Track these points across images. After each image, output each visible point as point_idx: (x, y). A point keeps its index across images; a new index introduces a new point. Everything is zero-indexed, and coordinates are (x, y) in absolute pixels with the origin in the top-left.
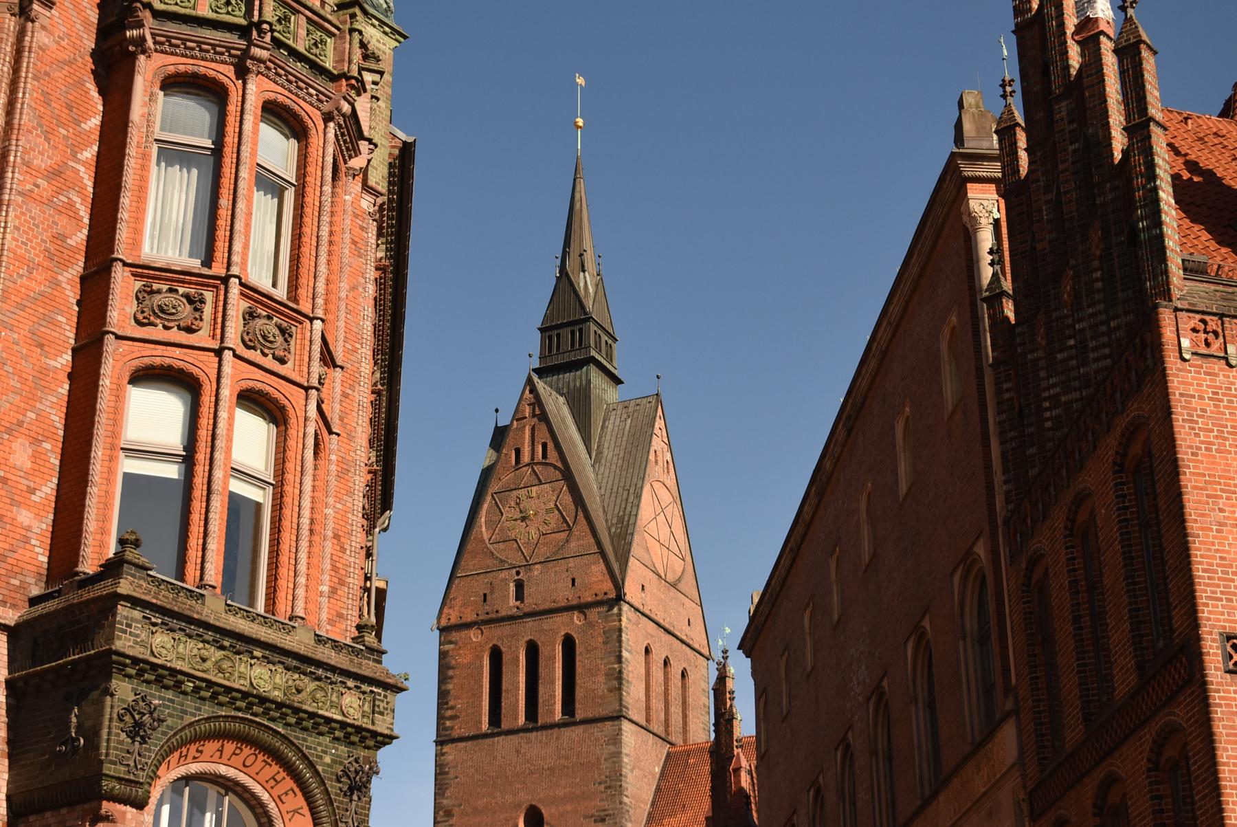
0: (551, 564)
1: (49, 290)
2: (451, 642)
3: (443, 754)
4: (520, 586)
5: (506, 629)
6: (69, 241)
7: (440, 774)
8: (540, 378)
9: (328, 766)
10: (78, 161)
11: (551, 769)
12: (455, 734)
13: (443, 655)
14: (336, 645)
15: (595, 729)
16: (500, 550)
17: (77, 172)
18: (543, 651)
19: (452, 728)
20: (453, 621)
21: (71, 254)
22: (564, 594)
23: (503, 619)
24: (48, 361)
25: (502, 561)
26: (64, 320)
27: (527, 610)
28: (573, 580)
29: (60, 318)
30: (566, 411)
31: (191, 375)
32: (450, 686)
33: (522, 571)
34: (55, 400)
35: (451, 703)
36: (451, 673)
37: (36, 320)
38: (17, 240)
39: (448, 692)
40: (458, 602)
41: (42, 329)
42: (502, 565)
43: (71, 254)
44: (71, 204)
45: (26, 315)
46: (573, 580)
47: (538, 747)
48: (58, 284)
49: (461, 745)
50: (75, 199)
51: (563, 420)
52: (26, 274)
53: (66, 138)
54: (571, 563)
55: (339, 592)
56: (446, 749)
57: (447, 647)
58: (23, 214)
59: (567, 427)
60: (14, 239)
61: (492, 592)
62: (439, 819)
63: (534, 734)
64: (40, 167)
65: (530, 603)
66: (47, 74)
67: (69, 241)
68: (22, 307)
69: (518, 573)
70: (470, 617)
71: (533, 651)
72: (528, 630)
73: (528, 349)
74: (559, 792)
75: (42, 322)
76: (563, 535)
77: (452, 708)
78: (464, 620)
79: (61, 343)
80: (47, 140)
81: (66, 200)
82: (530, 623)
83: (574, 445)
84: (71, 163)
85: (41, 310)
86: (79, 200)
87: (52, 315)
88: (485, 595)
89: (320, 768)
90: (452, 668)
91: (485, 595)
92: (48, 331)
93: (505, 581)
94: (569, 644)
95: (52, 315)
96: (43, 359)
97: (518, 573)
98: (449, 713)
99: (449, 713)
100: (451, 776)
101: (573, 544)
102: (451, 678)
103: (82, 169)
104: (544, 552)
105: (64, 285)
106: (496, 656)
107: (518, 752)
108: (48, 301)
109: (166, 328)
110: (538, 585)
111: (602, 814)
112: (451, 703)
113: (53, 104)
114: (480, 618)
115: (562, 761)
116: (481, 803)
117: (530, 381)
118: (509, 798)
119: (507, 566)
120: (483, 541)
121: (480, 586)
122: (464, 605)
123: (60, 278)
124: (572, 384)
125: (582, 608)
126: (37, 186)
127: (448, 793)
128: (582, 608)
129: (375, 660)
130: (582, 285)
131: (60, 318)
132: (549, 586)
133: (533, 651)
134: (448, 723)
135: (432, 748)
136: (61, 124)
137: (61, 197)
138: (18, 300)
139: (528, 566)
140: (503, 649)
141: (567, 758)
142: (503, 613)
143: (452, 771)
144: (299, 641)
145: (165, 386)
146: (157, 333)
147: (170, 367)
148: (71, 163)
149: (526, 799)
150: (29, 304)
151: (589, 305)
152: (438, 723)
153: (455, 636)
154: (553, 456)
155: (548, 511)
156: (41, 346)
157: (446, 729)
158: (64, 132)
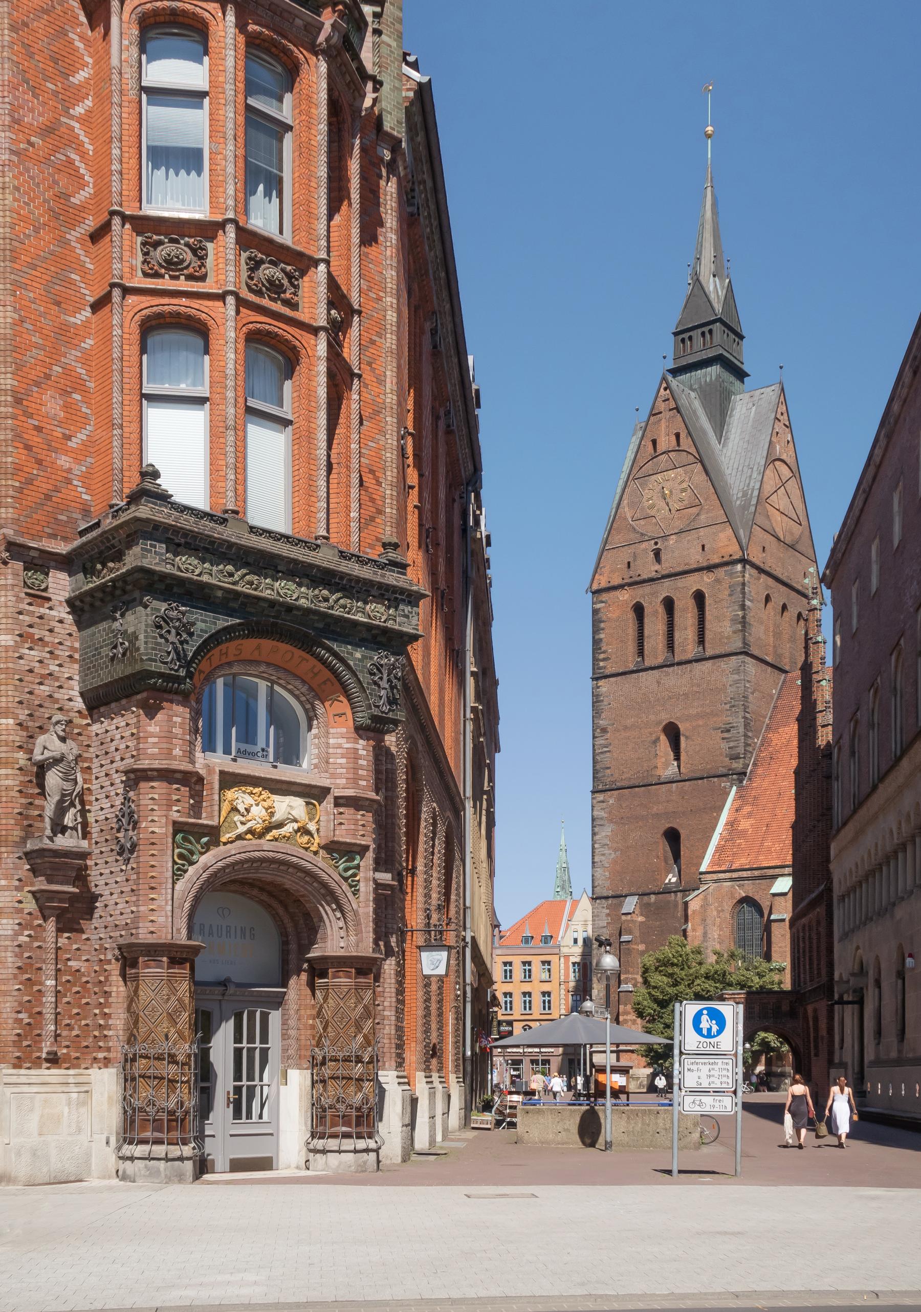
0: (683, 535)
1: (59, 249)
2: (602, 602)
3: (598, 687)
4: (657, 554)
5: (647, 589)
6: (72, 200)
7: (597, 702)
8: (674, 377)
9: (359, 660)
10: (72, 117)
11: (686, 695)
12: (608, 671)
13: (595, 612)
14: (360, 560)
15: (723, 664)
16: (640, 525)
17: (72, 129)
18: (678, 605)
19: (605, 667)
20: (604, 584)
21: (77, 213)
22: (695, 558)
23: (644, 581)
24: (68, 318)
25: (642, 534)
26: (78, 278)
27: (664, 573)
28: (703, 546)
29: (73, 276)
30: (697, 404)
31: (199, 321)
32: (602, 636)
33: (659, 541)
34: (79, 354)
35: (603, 649)
36: (602, 625)
37: (49, 279)
38: (19, 201)
39: (601, 640)
40: (606, 570)
41: (57, 287)
42: (643, 538)
43: (77, 213)
44: (71, 162)
45: (39, 274)
46: (703, 546)
47: (675, 679)
48: (67, 243)
49: (612, 679)
50: (73, 156)
51: (695, 412)
52: (33, 233)
53: (56, 93)
54: (702, 532)
55: (377, 520)
56: (601, 683)
57: (598, 606)
58: (21, 174)
59: (697, 418)
60: (15, 200)
61: (635, 560)
62: (597, 735)
63: (672, 668)
64: (32, 125)
65: (667, 566)
66: (26, 25)
67: (72, 200)
68: (34, 267)
69: (656, 543)
70: (617, 581)
71: (669, 604)
72: (665, 589)
73: (664, 351)
74: (693, 711)
75: (54, 280)
76: (694, 510)
77: (604, 652)
78: (611, 584)
79: (78, 300)
80: (35, 96)
81: (64, 158)
82: (667, 583)
83: (704, 433)
84: (63, 119)
85: (53, 268)
86: (77, 158)
87: (66, 274)
88: (629, 563)
89: (351, 663)
90: (603, 622)
91: (629, 563)
92: (64, 289)
93: (645, 550)
94: (699, 598)
95: (66, 274)
96: (63, 316)
97: (656, 543)
98: (602, 656)
99: (602, 656)
100: (605, 703)
101: (702, 517)
102: (603, 629)
103: (77, 125)
104: (679, 525)
105: (73, 244)
106: (639, 610)
107: (658, 683)
108: (59, 260)
109: (173, 278)
110: (673, 552)
111: (728, 726)
112: (603, 649)
113: (37, 57)
114: (626, 581)
115: (695, 689)
116: (629, 722)
117: (664, 379)
118: (652, 717)
119: (646, 538)
120: (625, 519)
121: (625, 555)
122: (612, 571)
123: (68, 236)
124: (703, 380)
125: (710, 568)
126: (32, 144)
127: (603, 716)
128: (710, 568)
129: (398, 573)
130: (711, 288)
131: (73, 276)
132: (683, 552)
133: (669, 604)
134: (601, 664)
135: (589, 684)
136: (47, 78)
137: (58, 155)
138: (29, 260)
139: (665, 537)
140: (645, 605)
141: (699, 686)
142: (645, 576)
143: (606, 699)
144: (324, 558)
145: (173, 331)
146: (166, 283)
147: (178, 314)
148: (63, 119)
149: (665, 718)
150: (39, 264)
151: (718, 307)
152: (593, 664)
153: (604, 596)
154: (686, 443)
155: (683, 490)
156: (58, 304)
157: (600, 668)
158: (53, 87)
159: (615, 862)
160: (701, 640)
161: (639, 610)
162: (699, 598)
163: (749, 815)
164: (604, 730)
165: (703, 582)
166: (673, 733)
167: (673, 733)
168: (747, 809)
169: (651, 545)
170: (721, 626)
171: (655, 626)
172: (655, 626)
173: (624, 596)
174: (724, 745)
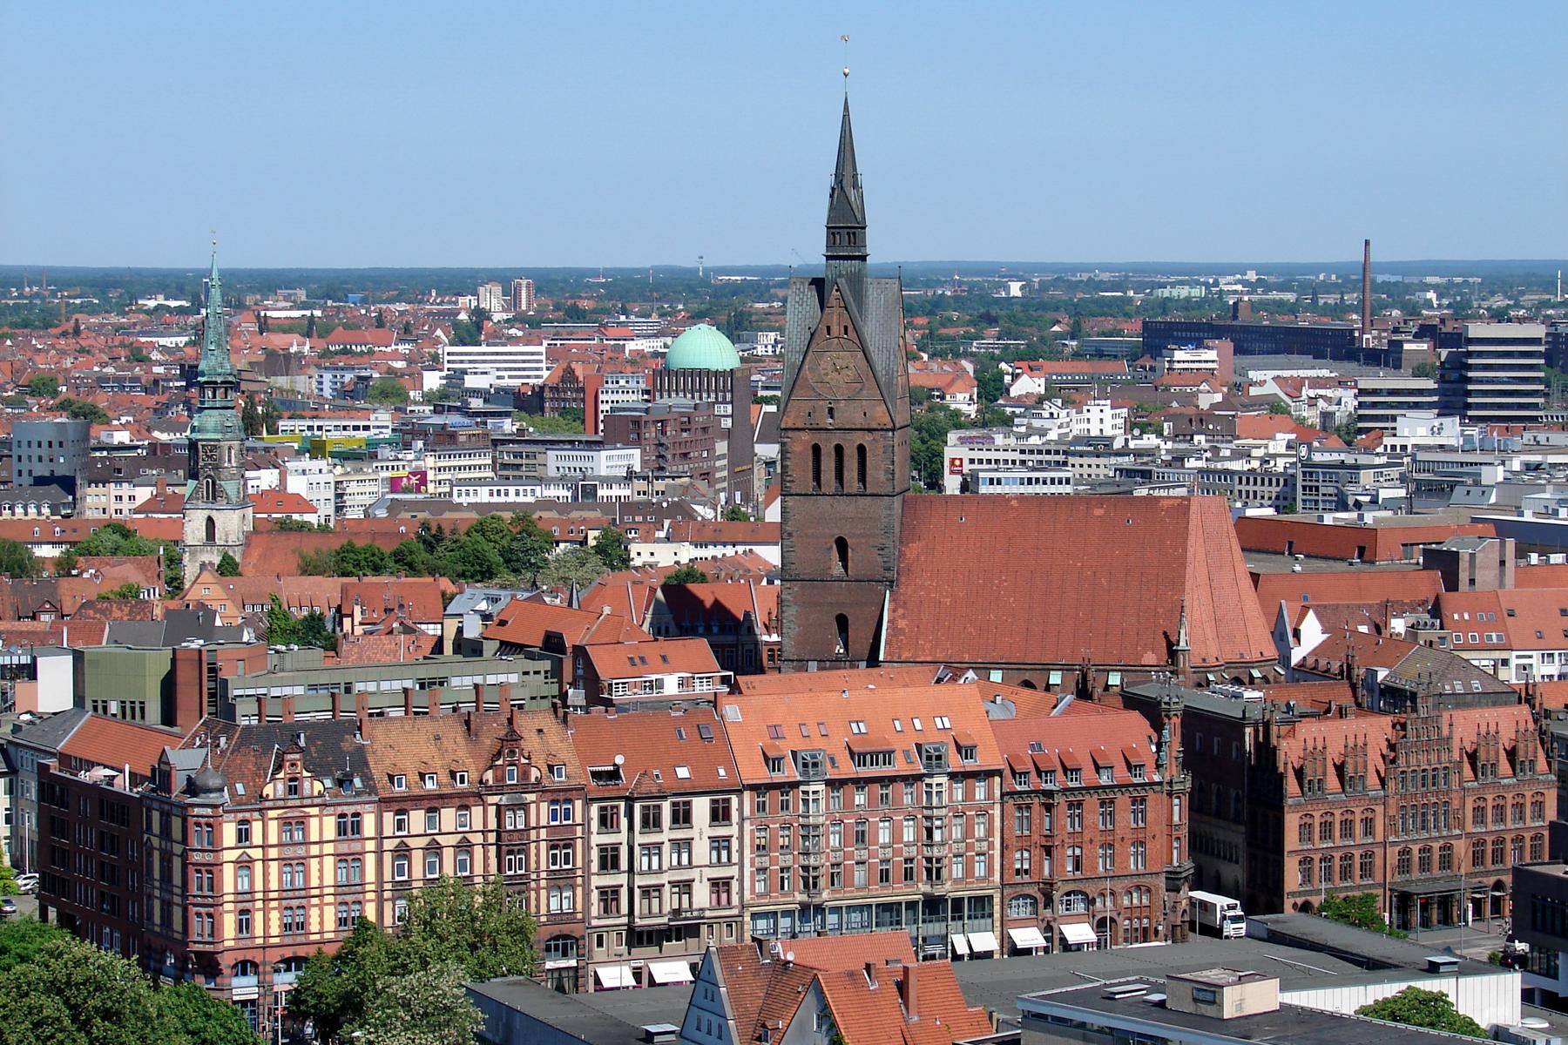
4: (831, 411)
5: (823, 435)
20: (790, 425)
22: (859, 421)
40: (793, 414)
70: (800, 425)
71: (839, 450)
72: (837, 439)
94: (861, 450)
106: (816, 450)
116: (810, 531)
121: (807, 407)
125: (870, 430)
132: (850, 414)
133: (839, 450)
142: (821, 425)
149: (837, 533)
159: (799, 634)
160: (862, 477)
161: (816, 450)
162: (861, 450)
163: (903, 617)
164: (790, 535)
165: (866, 439)
166: (842, 545)
167: (842, 545)
168: (901, 611)
169: (826, 404)
170: (876, 472)
171: (828, 464)
172: (828, 464)
173: (805, 436)
174: (880, 559)
